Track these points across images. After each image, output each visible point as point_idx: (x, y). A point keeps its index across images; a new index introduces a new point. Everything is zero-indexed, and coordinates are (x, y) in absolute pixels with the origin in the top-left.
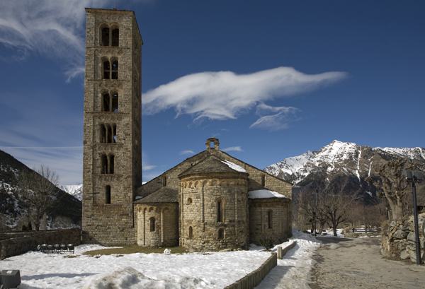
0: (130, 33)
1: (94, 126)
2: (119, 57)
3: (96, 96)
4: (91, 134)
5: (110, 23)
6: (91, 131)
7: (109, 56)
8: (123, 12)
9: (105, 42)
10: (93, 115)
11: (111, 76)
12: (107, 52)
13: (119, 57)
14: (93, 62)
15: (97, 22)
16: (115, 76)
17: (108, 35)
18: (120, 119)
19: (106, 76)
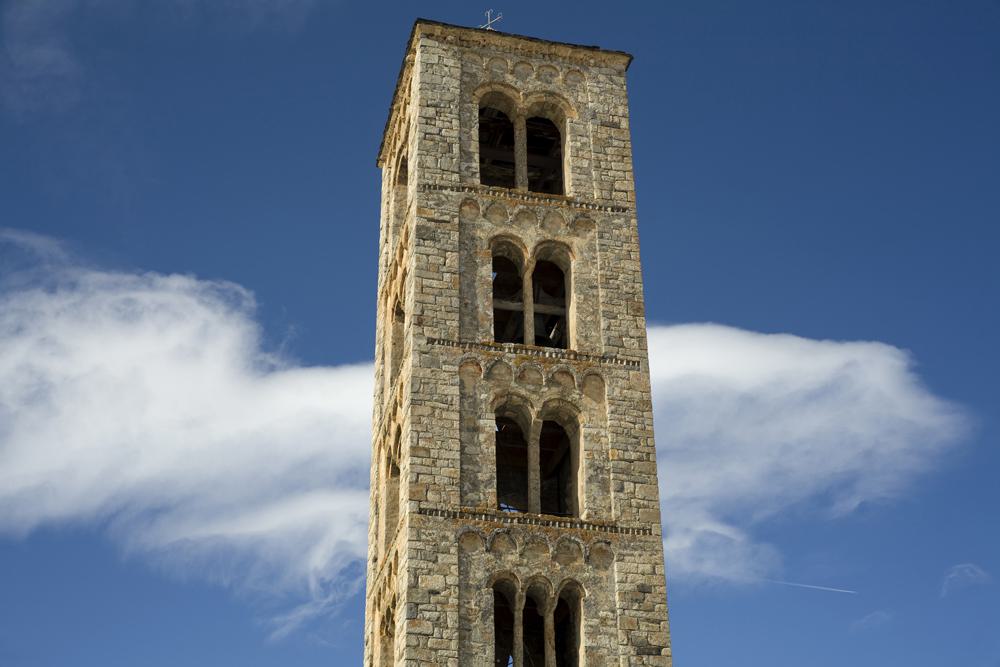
0: (621, 141)
1: (464, 586)
2: (577, 243)
3: (470, 429)
4: (451, 633)
5: (525, 90)
6: (452, 619)
7: (529, 238)
8: (581, 55)
9: (496, 171)
10: (460, 525)
11: (530, 333)
12: (517, 218)
13: (577, 243)
14: (452, 259)
15: (467, 83)
16: (552, 332)
17: (510, 141)
18: (600, 556)
19: (507, 327)
